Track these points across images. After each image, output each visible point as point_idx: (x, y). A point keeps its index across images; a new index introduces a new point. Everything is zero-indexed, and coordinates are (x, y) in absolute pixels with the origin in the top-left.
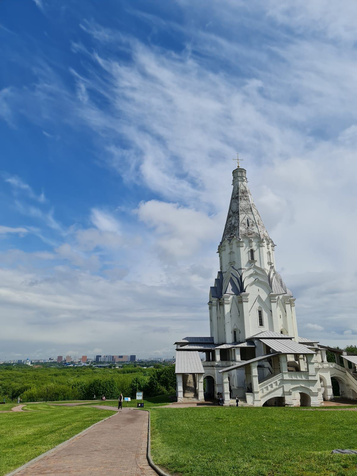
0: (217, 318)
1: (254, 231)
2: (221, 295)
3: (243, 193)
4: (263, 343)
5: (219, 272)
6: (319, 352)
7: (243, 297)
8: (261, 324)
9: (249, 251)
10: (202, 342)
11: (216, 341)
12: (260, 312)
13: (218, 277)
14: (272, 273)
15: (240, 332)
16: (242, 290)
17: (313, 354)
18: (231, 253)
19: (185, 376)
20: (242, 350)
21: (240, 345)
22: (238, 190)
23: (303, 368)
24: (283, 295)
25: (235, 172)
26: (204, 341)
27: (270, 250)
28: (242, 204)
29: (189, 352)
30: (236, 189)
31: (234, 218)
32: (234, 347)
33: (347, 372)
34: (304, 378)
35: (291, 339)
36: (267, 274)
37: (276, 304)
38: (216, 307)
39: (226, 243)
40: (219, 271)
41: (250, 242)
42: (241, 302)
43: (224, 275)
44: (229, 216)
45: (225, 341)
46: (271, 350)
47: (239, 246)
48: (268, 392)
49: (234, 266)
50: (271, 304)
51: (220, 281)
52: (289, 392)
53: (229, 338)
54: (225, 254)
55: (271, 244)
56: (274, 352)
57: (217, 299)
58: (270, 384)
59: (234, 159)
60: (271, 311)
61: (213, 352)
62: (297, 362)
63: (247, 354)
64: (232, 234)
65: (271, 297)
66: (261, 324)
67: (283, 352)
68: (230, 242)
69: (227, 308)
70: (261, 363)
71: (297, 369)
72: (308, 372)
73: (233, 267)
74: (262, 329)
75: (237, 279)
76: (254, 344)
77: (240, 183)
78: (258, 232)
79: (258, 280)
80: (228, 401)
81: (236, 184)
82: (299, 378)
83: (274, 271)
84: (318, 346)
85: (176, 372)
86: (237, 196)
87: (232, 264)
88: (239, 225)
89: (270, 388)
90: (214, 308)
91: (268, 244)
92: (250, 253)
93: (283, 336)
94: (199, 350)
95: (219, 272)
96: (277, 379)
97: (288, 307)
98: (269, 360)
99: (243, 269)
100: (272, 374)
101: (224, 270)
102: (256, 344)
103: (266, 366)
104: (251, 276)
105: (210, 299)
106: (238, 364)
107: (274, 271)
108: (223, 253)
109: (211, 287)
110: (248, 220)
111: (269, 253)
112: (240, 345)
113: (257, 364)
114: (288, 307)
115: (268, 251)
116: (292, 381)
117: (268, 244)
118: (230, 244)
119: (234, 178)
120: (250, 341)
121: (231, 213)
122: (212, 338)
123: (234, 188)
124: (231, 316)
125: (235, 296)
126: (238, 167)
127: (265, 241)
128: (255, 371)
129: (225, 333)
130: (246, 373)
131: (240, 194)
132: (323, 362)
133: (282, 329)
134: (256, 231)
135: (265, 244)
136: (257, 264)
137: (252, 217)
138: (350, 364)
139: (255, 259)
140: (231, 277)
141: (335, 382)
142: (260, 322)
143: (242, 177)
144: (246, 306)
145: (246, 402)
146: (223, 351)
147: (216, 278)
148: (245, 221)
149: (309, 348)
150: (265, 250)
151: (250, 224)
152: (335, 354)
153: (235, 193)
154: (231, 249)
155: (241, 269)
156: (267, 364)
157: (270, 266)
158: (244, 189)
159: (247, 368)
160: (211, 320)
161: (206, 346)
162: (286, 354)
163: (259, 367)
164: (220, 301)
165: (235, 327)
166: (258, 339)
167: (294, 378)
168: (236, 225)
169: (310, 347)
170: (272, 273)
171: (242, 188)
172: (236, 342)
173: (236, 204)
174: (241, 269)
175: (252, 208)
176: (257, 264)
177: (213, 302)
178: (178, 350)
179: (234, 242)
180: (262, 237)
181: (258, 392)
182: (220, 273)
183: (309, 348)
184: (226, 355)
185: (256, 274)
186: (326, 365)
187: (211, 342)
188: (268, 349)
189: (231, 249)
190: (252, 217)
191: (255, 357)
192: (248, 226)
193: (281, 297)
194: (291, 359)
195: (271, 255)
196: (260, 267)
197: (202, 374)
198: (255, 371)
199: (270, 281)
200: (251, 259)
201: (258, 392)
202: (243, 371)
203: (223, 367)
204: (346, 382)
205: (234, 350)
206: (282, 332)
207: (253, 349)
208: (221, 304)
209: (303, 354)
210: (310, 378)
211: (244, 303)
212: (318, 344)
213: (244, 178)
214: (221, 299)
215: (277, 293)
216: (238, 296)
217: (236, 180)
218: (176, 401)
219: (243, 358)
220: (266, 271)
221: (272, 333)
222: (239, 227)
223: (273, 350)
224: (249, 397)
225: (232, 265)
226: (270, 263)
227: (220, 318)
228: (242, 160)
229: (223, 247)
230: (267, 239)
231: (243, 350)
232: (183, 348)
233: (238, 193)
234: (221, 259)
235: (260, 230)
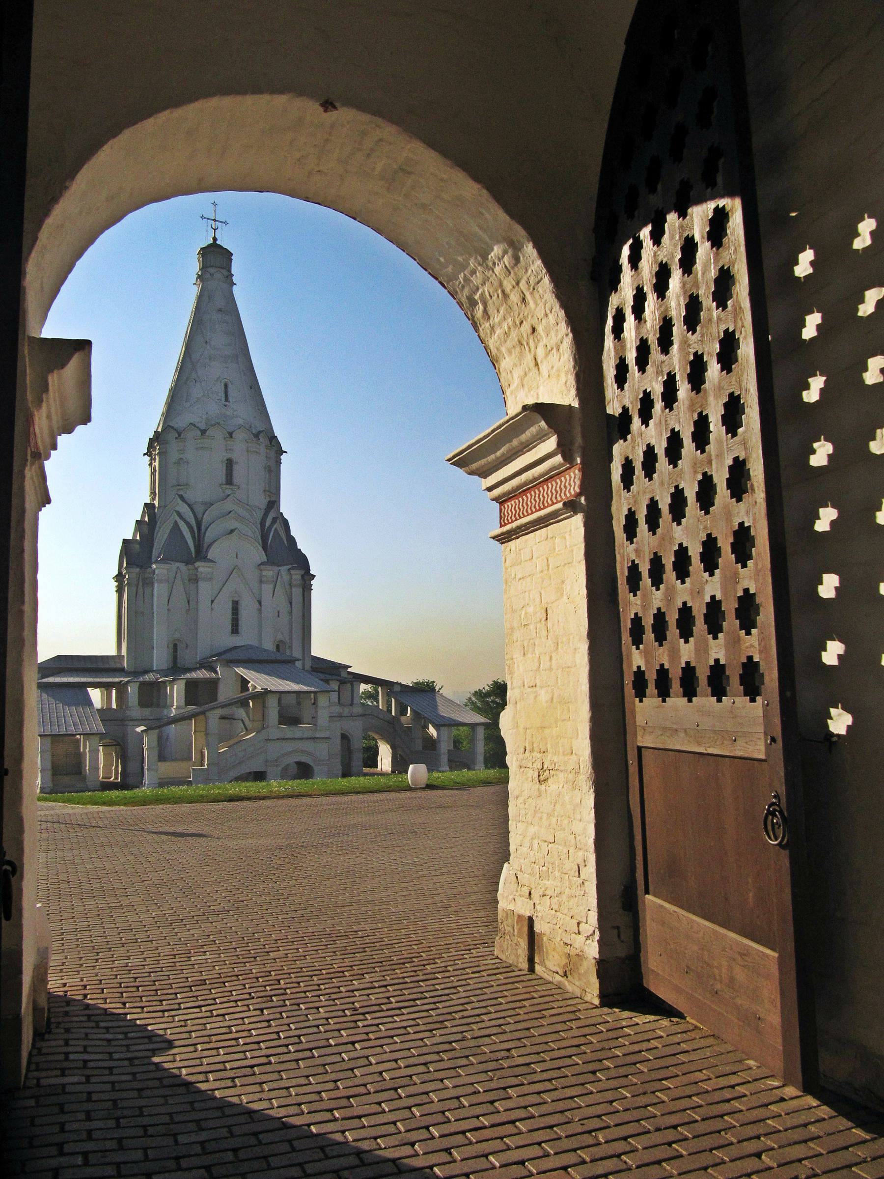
5: (146, 504)
7: (200, 570)
13: (143, 516)
14: (271, 515)
15: (187, 647)
16: (201, 553)
19: (55, 739)
26: (100, 665)
42: (194, 580)
46: (249, 685)
49: (184, 495)
52: (276, 761)
59: (203, 217)
60: (260, 602)
65: (264, 573)
66: (235, 629)
68: (179, 435)
69: (159, 590)
73: (181, 497)
76: (216, 672)
84: (350, 673)
92: (225, 465)
93: (279, 657)
95: (146, 504)
110: (226, 386)
125: (182, 566)
126: (215, 239)
133: (281, 641)
140: (176, 522)
142: (233, 626)
144: (205, 589)
152: (380, 689)
154: (182, 451)
157: (268, 499)
164: (147, 575)
167: (289, 735)
192: (227, 400)
200: (227, 481)
208: (148, 582)
211: (200, 582)
212: (349, 670)
214: (149, 570)
216: (190, 567)
228: (226, 223)
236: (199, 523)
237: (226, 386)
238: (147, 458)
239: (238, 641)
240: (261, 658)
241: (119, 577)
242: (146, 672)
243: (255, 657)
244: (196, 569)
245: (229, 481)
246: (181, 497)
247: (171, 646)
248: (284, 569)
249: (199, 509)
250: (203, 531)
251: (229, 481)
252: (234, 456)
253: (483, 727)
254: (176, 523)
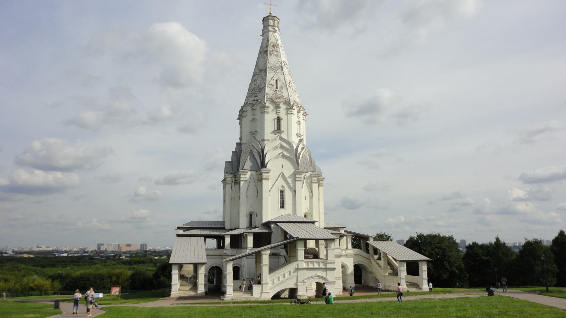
1: (283, 94)
2: (238, 170)
3: (274, 46)
4: (281, 229)
6: (345, 237)
7: (264, 174)
8: (282, 206)
9: (274, 119)
10: (210, 226)
11: (227, 227)
12: (282, 192)
14: (301, 146)
16: (263, 165)
17: (334, 239)
18: (254, 120)
20: (256, 235)
21: (254, 230)
22: (268, 42)
23: (322, 255)
24: (309, 173)
25: (265, 20)
26: (213, 226)
28: (272, 60)
29: (192, 238)
30: (266, 41)
31: (260, 77)
32: (245, 232)
33: (371, 258)
34: (321, 266)
35: (313, 223)
36: (295, 147)
37: (301, 182)
38: (230, 185)
39: (249, 108)
40: (239, 141)
41: (277, 107)
42: (260, 180)
43: (242, 146)
44: (254, 75)
45: (239, 225)
47: (263, 112)
48: (279, 282)
50: (295, 184)
51: (237, 155)
53: (243, 222)
54: (247, 120)
55: (302, 112)
56: (291, 237)
57: (232, 176)
58: (282, 273)
59: (265, 4)
60: (295, 191)
61: (223, 238)
62: (317, 249)
63: (261, 240)
64: (256, 96)
65: (297, 176)
66: (282, 206)
67: (300, 238)
70: (275, 251)
71: (316, 256)
72: (327, 259)
74: (283, 212)
75: (259, 153)
77: (270, 33)
78: (287, 96)
79: (283, 154)
80: (230, 293)
81: (265, 35)
82: (316, 266)
83: (303, 144)
85: (171, 261)
86: (266, 49)
87: (253, 134)
88: (265, 86)
89: (281, 278)
90: (228, 187)
91: (298, 112)
92: (276, 121)
93: (305, 220)
94: (206, 237)
96: (291, 267)
97: (315, 186)
98: (285, 246)
99: (266, 140)
100: (287, 262)
101: (244, 141)
102: (273, 229)
103: (282, 254)
104: (275, 148)
105: (225, 175)
106: (248, 252)
107: (303, 144)
108: (244, 119)
109: (227, 162)
110: (276, 81)
111: (299, 123)
112: (254, 230)
113: (269, 252)
114: (315, 186)
115: (297, 120)
116: (308, 269)
117: (298, 112)
118: (253, 109)
119: (264, 27)
120: (267, 225)
121: (257, 70)
122: (223, 223)
123: (263, 40)
125: (254, 173)
127: (295, 107)
128: (265, 259)
129: (239, 217)
130: (256, 263)
131: (270, 48)
132: (347, 248)
133: (306, 213)
134: (285, 94)
135: (295, 111)
136: (284, 136)
137: (281, 77)
138: (376, 251)
139: (282, 129)
141: (358, 269)
143: (274, 26)
144: (266, 185)
145: (252, 294)
146: (233, 237)
147: (234, 151)
148: (273, 82)
149: (332, 234)
150: (294, 118)
151: (279, 86)
153: (265, 45)
154: (254, 115)
155: (264, 140)
156: (283, 252)
157: (299, 138)
158: (275, 42)
159: (258, 256)
160: (224, 202)
161: (214, 231)
162: (305, 241)
163: (272, 255)
164: (236, 179)
165: (252, 210)
166: (275, 223)
167: (311, 266)
168: (262, 86)
169: (334, 232)
170: (301, 146)
171: (272, 40)
172: (251, 226)
173: (263, 60)
174: (264, 140)
175: (283, 66)
176: (284, 136)
177: (228, 179)
178: (178, 236)
179: (258, 107)
180: (292, 103)
181: (267, 283)
182: (239, 145)
183: (332, 234)
184: (237, 241)
185: (282, 147)
186: (351, 251)
187: (222, 226)
188: (285, 233)
189: (254, 115)
190: (281, 77)
191: (270, 243)
192: (277, 88)
193: (308, 174)
194: (311, 245)
195: (301, 125)
196: (286, 138)
197: (203, 264)
198: (265, 259)
199: (297, 157)
201: (267, 283)
202: (252, 261)
203: (232, 256)
204: (370, 270)
205: (246, 235)
206: (305, 216)
207: (269, 235)
209: (325, 240)
210: (329, 266)
211: (264, 181)
212: (345, 229)
213: (276, 29)
214: (238, 176)
215: (303, 170)
216: (258, 173)
217: (267, 30)
218: (169, 295)
219: (255, 245)
220: (294, 144)
221: (293, 216)
222: (265, 89)
223: (290, 236)
224: (256, 289)
225: (254, 135)
226: (299, 135)
227: (234, 199)
228: (276, 5)
229: (244, 113)
230: (297, 106)
231: (256, 235)
232: (186, 233)
233: (267, 47)
234: (241, 128)
235: (290, 94)
236: (263, 150)
238: (239, 121)
240: (295, 220)
241: (224, 181)
242: (236, 229)
243: (292, 220)
244: (261, 174)
247: (249, 216)
250: (265, 153)
253: (425, 263)
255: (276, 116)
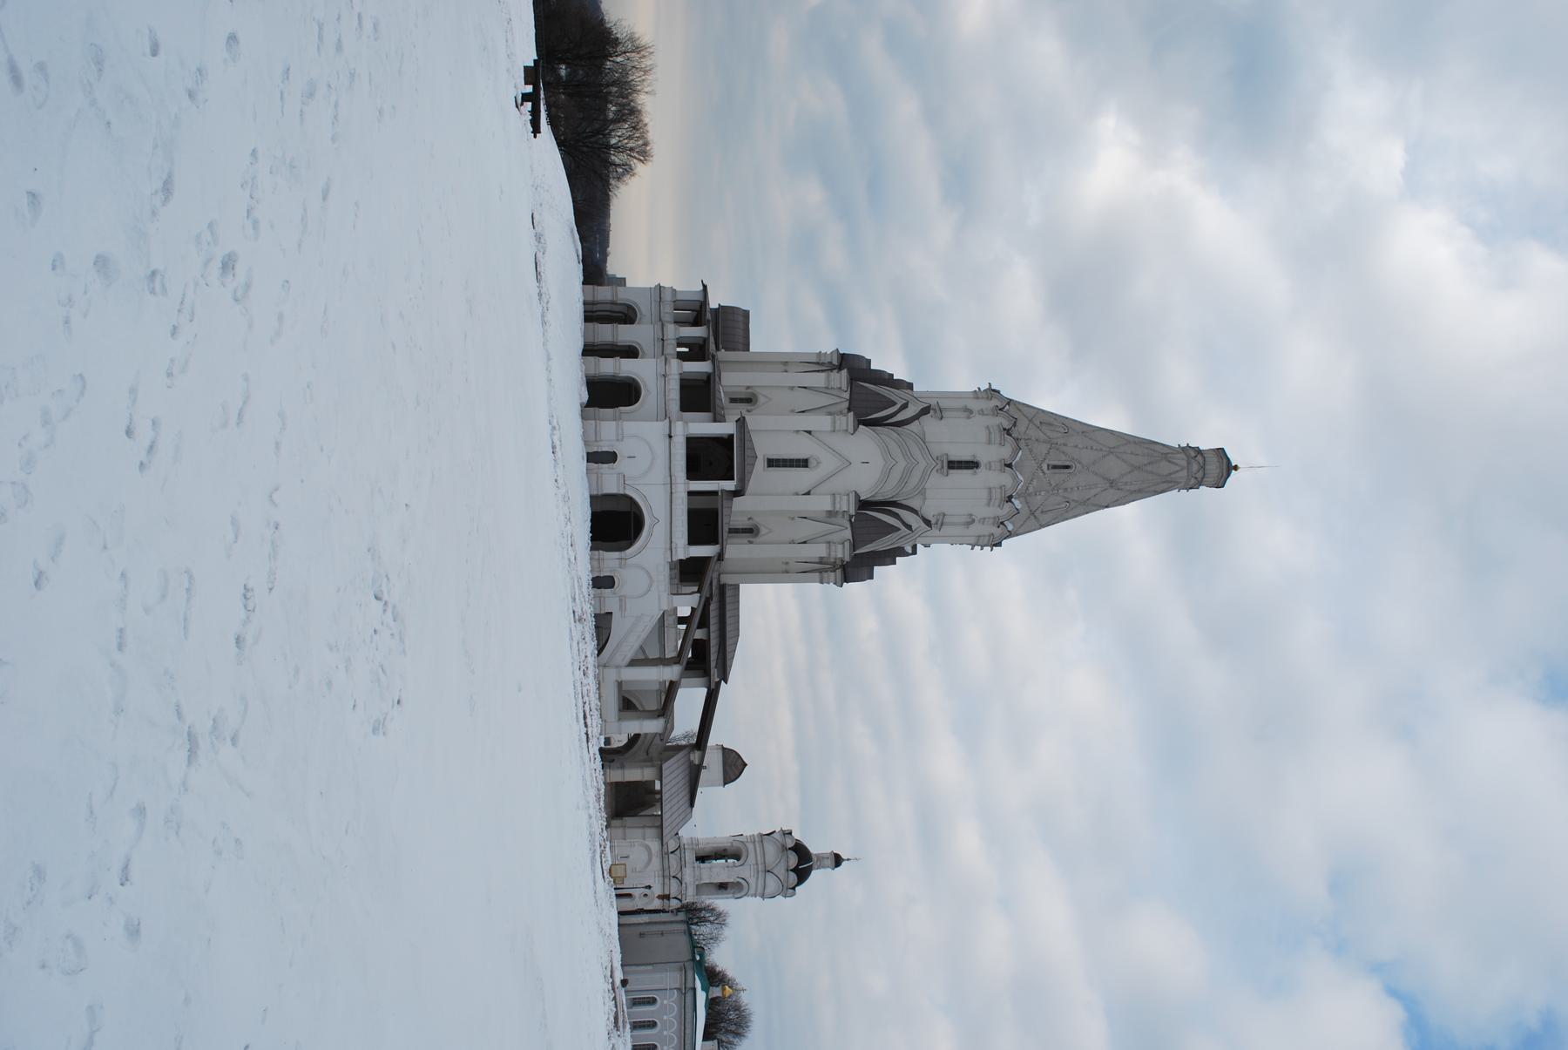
0: (786, 363)
8: (772, 463)
12: (803, 463)
25: (1220, 452)
27: (976, 529)
39: (995, 402)
55: (998, 532)
60: (808, 493)
66: (772, 463)
69: (819, 379)
97: (818, 551)
110: (1067, 467)
124: (792, 388)
126: (1236, 468)
154: (982, 412)
165: (762, 399)
189: (982, 412)
211: (829, 418)
237: (1067, 467)
239: (760, 464)
245: (954, 465)
246: (926, 411)
248: (848, 534)
249: (914, 426)
251: (954, 465)
252: (982, 471)
254: (894, 404)
255: (983, 458)
